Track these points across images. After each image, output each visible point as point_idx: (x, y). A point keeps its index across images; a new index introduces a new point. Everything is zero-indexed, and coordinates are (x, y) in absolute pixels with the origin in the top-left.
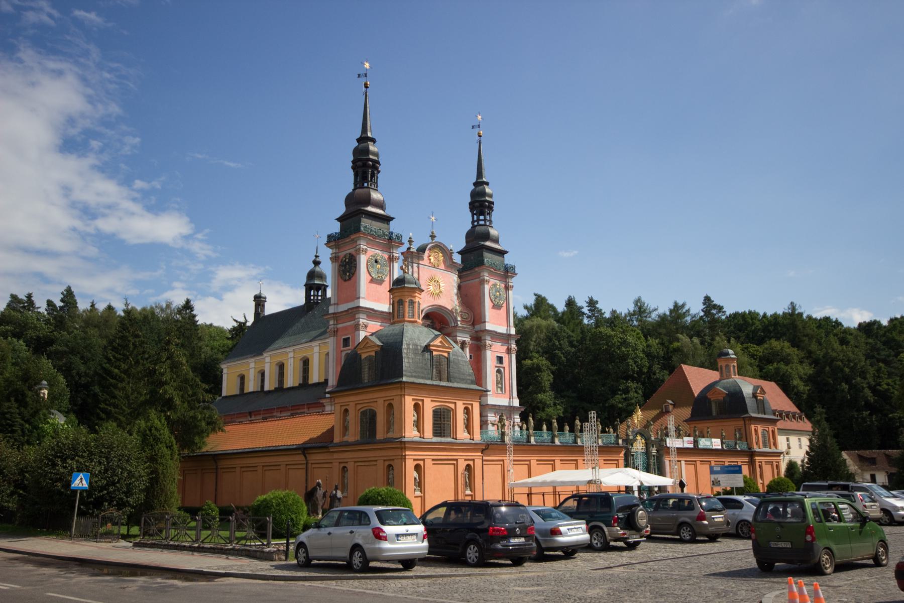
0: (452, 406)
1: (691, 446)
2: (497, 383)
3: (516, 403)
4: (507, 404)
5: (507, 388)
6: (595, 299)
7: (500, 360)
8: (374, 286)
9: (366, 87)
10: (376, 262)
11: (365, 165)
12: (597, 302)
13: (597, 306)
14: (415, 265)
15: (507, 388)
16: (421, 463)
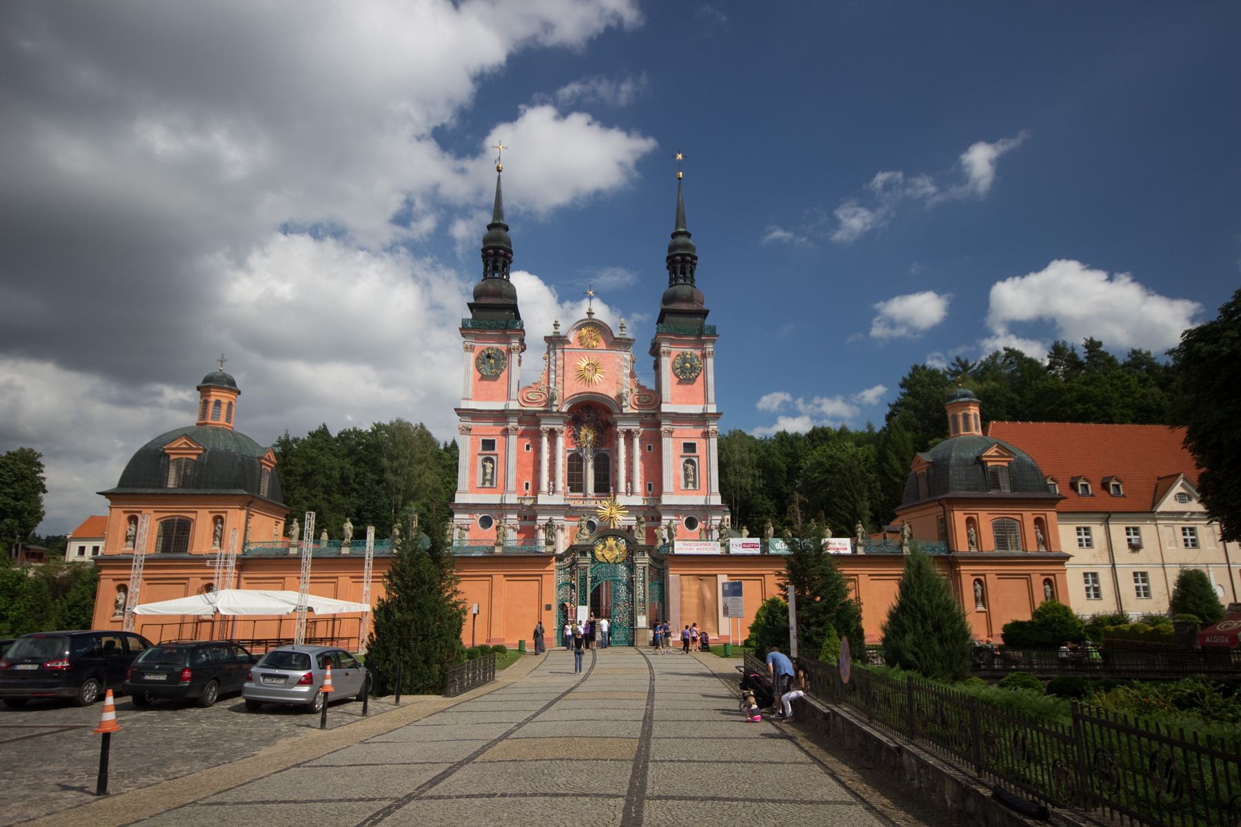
0: (192, 516)
1: (757, 551)
2: (687, 476)
3: (716, 500)
4: (703, 503)
5: (704, 482)
6: (1096, 339)
7: (690, 447)
8: (485, 383)
9: (499, 171)
10: (489, 356)
11: (496, 254)
12: (1100, 344)
13: (1102, 349)
14: (559, 351)
15: (704, 482)
16: (1052, 578)
